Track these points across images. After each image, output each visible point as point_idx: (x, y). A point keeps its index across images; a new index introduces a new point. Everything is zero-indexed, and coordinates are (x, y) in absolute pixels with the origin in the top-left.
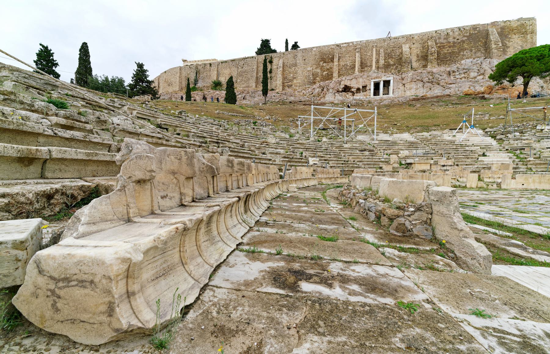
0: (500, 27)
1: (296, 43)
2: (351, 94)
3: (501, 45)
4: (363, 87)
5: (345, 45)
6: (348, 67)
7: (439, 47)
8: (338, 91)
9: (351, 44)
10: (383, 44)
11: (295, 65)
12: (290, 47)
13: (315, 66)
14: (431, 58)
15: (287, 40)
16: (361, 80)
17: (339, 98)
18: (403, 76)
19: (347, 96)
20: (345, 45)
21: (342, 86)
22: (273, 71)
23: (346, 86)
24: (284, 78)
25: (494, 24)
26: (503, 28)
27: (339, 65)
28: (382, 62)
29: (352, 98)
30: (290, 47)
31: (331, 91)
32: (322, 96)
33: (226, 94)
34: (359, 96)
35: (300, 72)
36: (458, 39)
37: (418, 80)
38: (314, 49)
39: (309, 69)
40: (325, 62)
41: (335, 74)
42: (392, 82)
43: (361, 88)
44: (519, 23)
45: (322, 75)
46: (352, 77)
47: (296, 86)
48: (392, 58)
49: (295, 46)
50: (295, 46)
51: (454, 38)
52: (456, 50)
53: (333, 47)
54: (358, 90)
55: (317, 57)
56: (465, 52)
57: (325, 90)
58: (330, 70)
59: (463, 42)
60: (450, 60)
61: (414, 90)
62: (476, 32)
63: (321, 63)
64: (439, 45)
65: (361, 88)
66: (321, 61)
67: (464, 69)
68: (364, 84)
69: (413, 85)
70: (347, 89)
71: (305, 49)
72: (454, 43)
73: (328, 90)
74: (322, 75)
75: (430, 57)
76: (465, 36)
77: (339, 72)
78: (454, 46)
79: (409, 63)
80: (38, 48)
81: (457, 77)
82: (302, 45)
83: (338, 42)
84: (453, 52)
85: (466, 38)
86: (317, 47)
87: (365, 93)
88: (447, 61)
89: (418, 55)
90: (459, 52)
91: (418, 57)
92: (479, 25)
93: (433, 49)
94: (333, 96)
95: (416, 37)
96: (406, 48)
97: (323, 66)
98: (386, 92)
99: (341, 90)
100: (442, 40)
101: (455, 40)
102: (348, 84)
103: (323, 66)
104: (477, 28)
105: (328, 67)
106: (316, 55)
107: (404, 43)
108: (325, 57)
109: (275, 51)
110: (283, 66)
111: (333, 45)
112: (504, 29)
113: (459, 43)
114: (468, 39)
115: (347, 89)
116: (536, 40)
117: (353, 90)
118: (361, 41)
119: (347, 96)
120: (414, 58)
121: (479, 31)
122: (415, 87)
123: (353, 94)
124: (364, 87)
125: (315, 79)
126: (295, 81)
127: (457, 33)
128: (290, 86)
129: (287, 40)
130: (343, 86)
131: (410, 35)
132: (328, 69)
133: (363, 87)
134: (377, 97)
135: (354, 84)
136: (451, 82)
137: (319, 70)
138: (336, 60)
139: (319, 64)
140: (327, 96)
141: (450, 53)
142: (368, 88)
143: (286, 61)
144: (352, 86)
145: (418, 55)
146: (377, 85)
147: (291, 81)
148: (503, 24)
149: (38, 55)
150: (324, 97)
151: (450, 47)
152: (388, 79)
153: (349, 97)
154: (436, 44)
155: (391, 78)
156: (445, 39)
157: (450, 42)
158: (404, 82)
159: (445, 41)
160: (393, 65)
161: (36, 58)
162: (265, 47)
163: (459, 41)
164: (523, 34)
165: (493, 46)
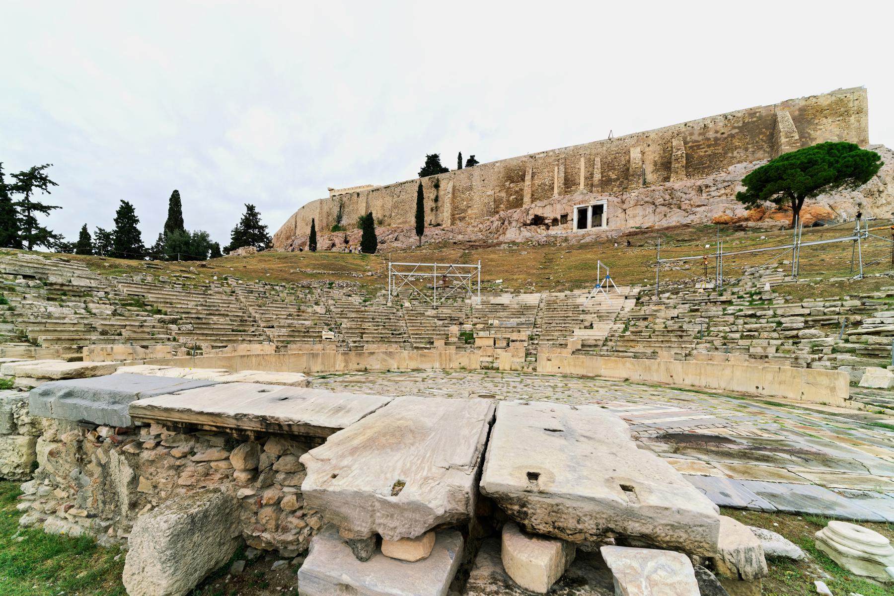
0: (797, 107)
1: (472, 157)
2: (544, 227)
3: (797, 137)
4: (562, 216)
5: (542, 155)
6: (547, 187)
7: (691, 147)
8: (525, 225)
9: (551, 153)
10: (600, 150)
11: (470, 188)
12: (464, 163)
13: (498, 189)
14: (677, 165)
15: (460, 154)
16: (558, 206)
17: (526, 233)
18: (624, 197)
19: (539, 230)
20: (542, 155)
21: (531, 217)
22: (440, 199)
23: (536, 216)
24: (455, 208)
25: (786, 104)
26: (803, 110)
27: (533, 185)
28: (597, 177)
29: (545, 233)
30: (464, 163)
31: (514, 224)
32: (501, 232)
33: (363, 236)
34: (557, 231)
35: (476, 198)
36: (723, 133)
37: (647, 202)
38: (497, 165)
39: (490, 193)
40: (512, 182)
41: (527, 199)
42: (605, 207)
43: (559, 218)
44: (834, 98)
45: (508, 201)
46: (545, 202)
47: (471, 218)
48: (615, 169)
49: (472, 162)
50: (472, 162)
51: (717, 132)
52: (720, 151)
53: (524, 159)
54: (555, 222)
55: (501, 175)
56: (735, 152)
57: (506, 223)
58: (520, 193)
59: (732, 136)
60: (709, 167)
61: (640, 218)
62: (755, 119)
63: (507, 183)
64: (690, 144)
65: (559, 218)
66: (506, 181)
67: (724, 181)
68: (563, 213)
69: (639, 210)
70: (538, 221)
71: (485, 165)
72: (716, 139)
73: (510, 223)
74: (508, 201)
75: (675, 165)
76: (735, 128)
77: (533, 195)
79: (640, 176)
80: (118, 206)
81: (713, 194)
82: (481, 159)
83: (531, 152)
84: (715, 154)
85: (737, 131)
86: (501, 161)
87: (565, 225)
88: (705, 168)
89: (655, 162)
90: (726, 153)
91: (655, 165)
92: (759, 108)
93: (680, 152)
94: (518, 232)
95: (652, 136)
96: (635, 154)
97: (509, 188)
98: (597, 223)
99: (528, 222)
100: (696, 137)
101: (719, 135)
102: (539, 212)
103: (509, 188)
104: (756, 113)
105: (517, 189)
106: (500, 172)
107: (634, 146)
108: (512, 175)
109: (446, 170)
110: (454, 190)
111: (525, 156)
112: (805, 110)
113: (726, 138)
114: (741, 132)
115: (538, 221)
116: (867, 124)
117: (547, 221)
118: (566, 148)
119: (539, 230)
120: (649, 168)
121: (760, 118)
122: (641, 214)
124: (564, 217)
125: (498, 207)
126: (470, 211)
127: (721, 124)
128: (462, 219)
129: (460, 154)
130: (533, 217)
131: (643, 133)
132: (517, 192)
133: (562, 216)
134: (583, 231)
135: (549, 213)
136: (699, 203)
137: (503, 194)
138: (528, 177)
139: (504, 185)
140: (508, 232)
141: (710, 156)
142: (569, 218)
143: (457, 184)
144: (545, 215)
145: (655, 162)
146: (583, 213)
147: (464, 211)
148: (803, 103)
149: (118, 212)
150: (504, 233)
151: (709, 146)
152: (599, 203)
153: (540, 234)
154: (686, 143)
155: (604, 202)
156: (700, 134)
157: (709, 139)
158: (624, 207)
159: (701, 138)
160: (618, 179)
161: (116, 216)
162: (433, 166)
163: (724, 136)
165: (783, 140)
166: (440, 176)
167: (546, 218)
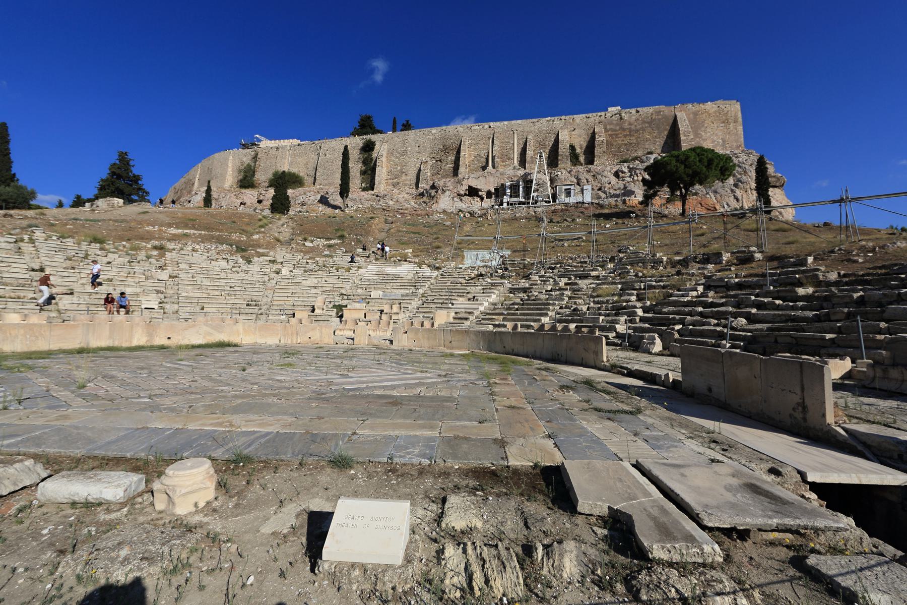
2: (478, 199)
16: (491, 179)
17: (459, 204)
23: (470, 187)
31: (447, 193)
43: (493, 191)
54: (489, 194)
57: (440, 192)
65: (493, 191)
73: (444, 191)
78: (630, 135)
102: (473, 185)
117: (480, 193)
123: (482, 199)
126: (404, 178)
140: (441, 201)
141: (626, 145)
144: (479, 187)
157: (624, 130)
164: (724, 122)
165: (682, 137)
167: (480, 190)
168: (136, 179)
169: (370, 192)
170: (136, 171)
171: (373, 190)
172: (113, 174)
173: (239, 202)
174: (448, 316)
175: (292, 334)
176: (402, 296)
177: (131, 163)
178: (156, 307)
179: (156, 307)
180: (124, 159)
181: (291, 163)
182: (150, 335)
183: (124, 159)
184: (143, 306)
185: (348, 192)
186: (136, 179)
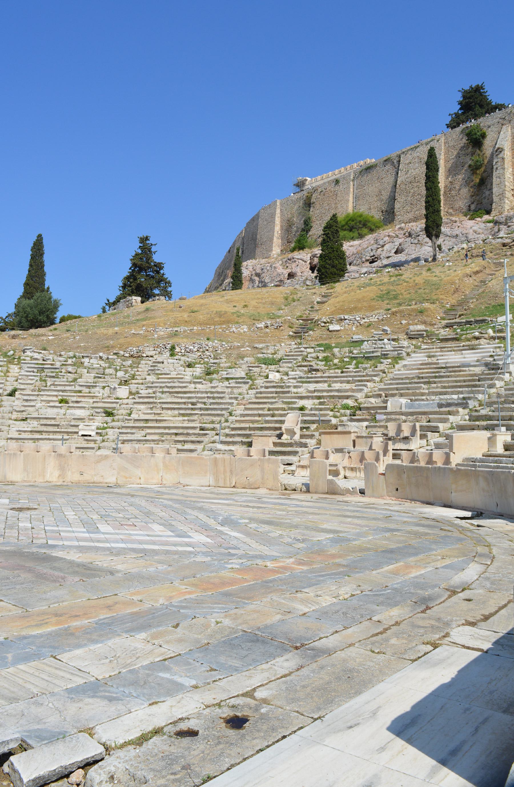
166: (486, 122)
168: (159, 266)
169: (486, 217)
170: (156, 258)
171: (488, 212)
172: (134, 265)
173: (286, 272)
174: (491, 440)
175: (225, 471)
176: (440, 406)
177: (153, 249)
178: (93, 433)
179: (93, 433)
180: (145, 247)
181: (356, 198)
182: (62, 469)
183: (145, 247)
184: (81, 433)
185: (439, 226)
186: (159, 266)
